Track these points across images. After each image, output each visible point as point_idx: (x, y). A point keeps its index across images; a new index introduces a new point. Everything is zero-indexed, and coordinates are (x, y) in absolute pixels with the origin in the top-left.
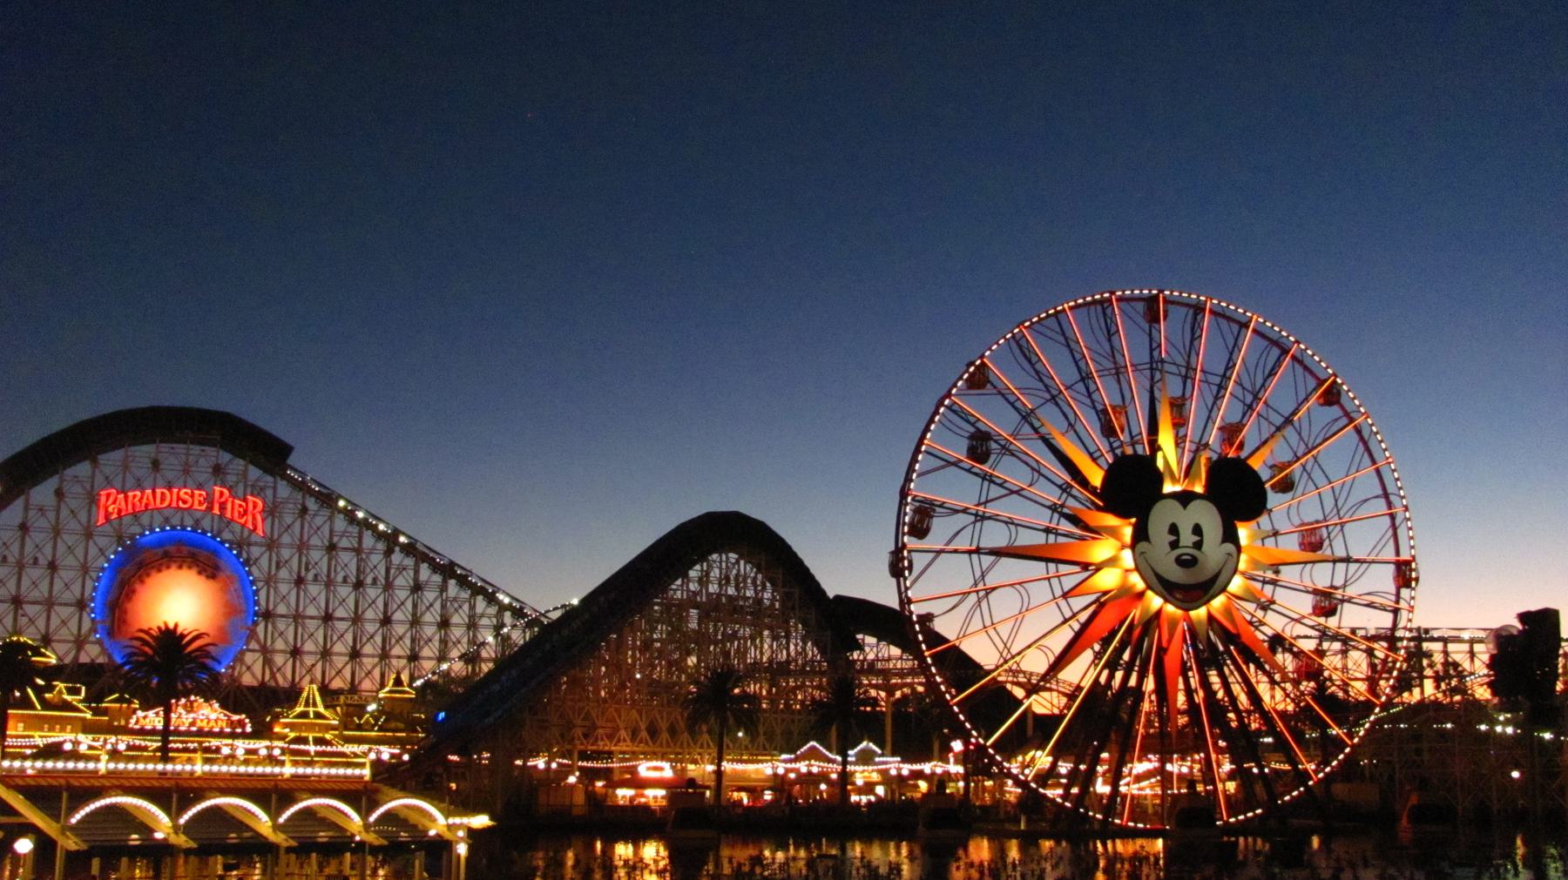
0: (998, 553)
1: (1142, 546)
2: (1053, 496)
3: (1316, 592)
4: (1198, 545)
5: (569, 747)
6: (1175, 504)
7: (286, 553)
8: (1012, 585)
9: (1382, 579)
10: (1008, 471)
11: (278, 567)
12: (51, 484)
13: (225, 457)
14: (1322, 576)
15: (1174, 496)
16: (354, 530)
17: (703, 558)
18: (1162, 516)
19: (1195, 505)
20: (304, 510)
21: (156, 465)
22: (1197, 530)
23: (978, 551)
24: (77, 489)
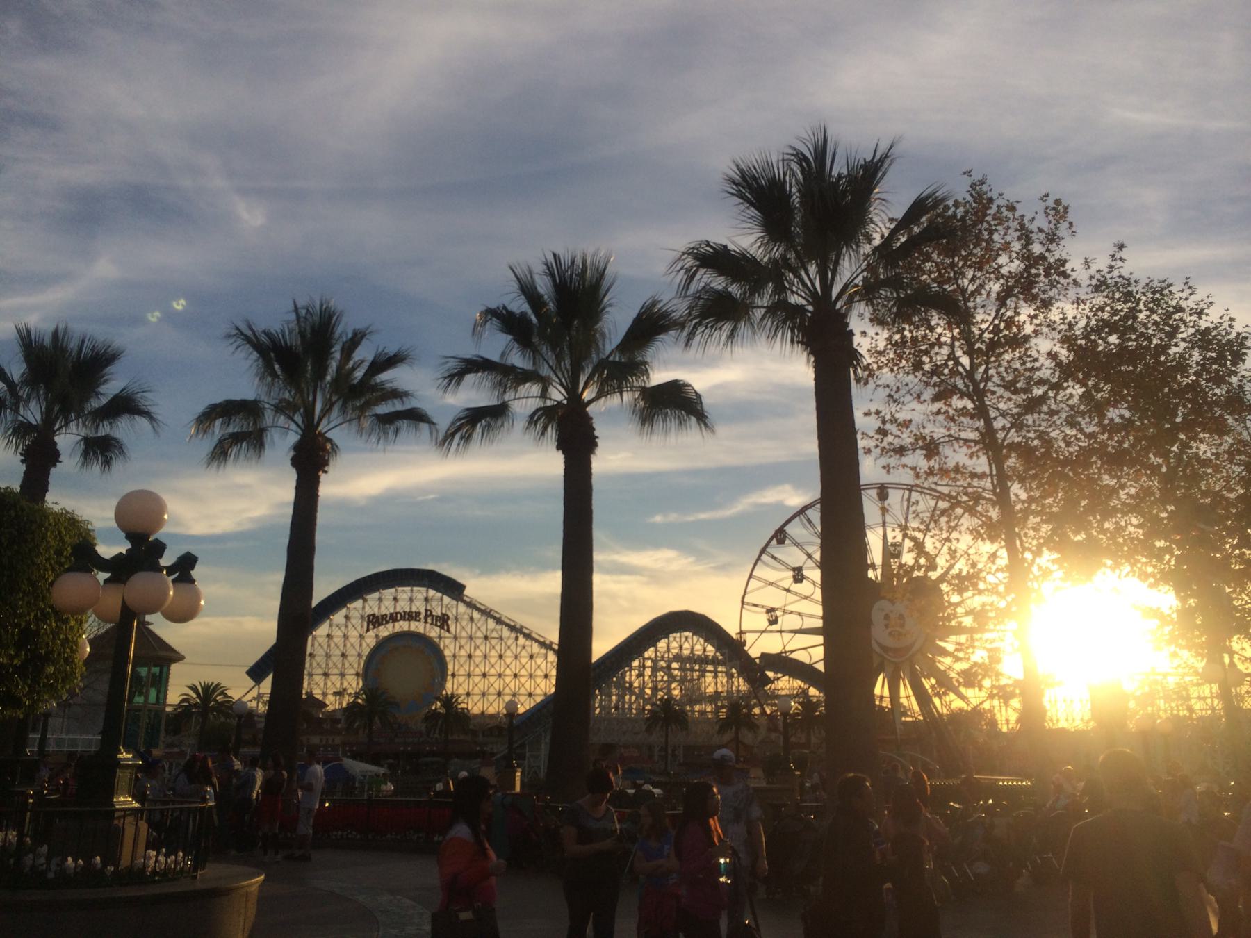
0: (795, 632)
7: (463, 642)
12: (343, 612)
13: (432, 592)
16: (499, 627)
17: (667, 636)
20: (472, 619)
21: (395, 599)
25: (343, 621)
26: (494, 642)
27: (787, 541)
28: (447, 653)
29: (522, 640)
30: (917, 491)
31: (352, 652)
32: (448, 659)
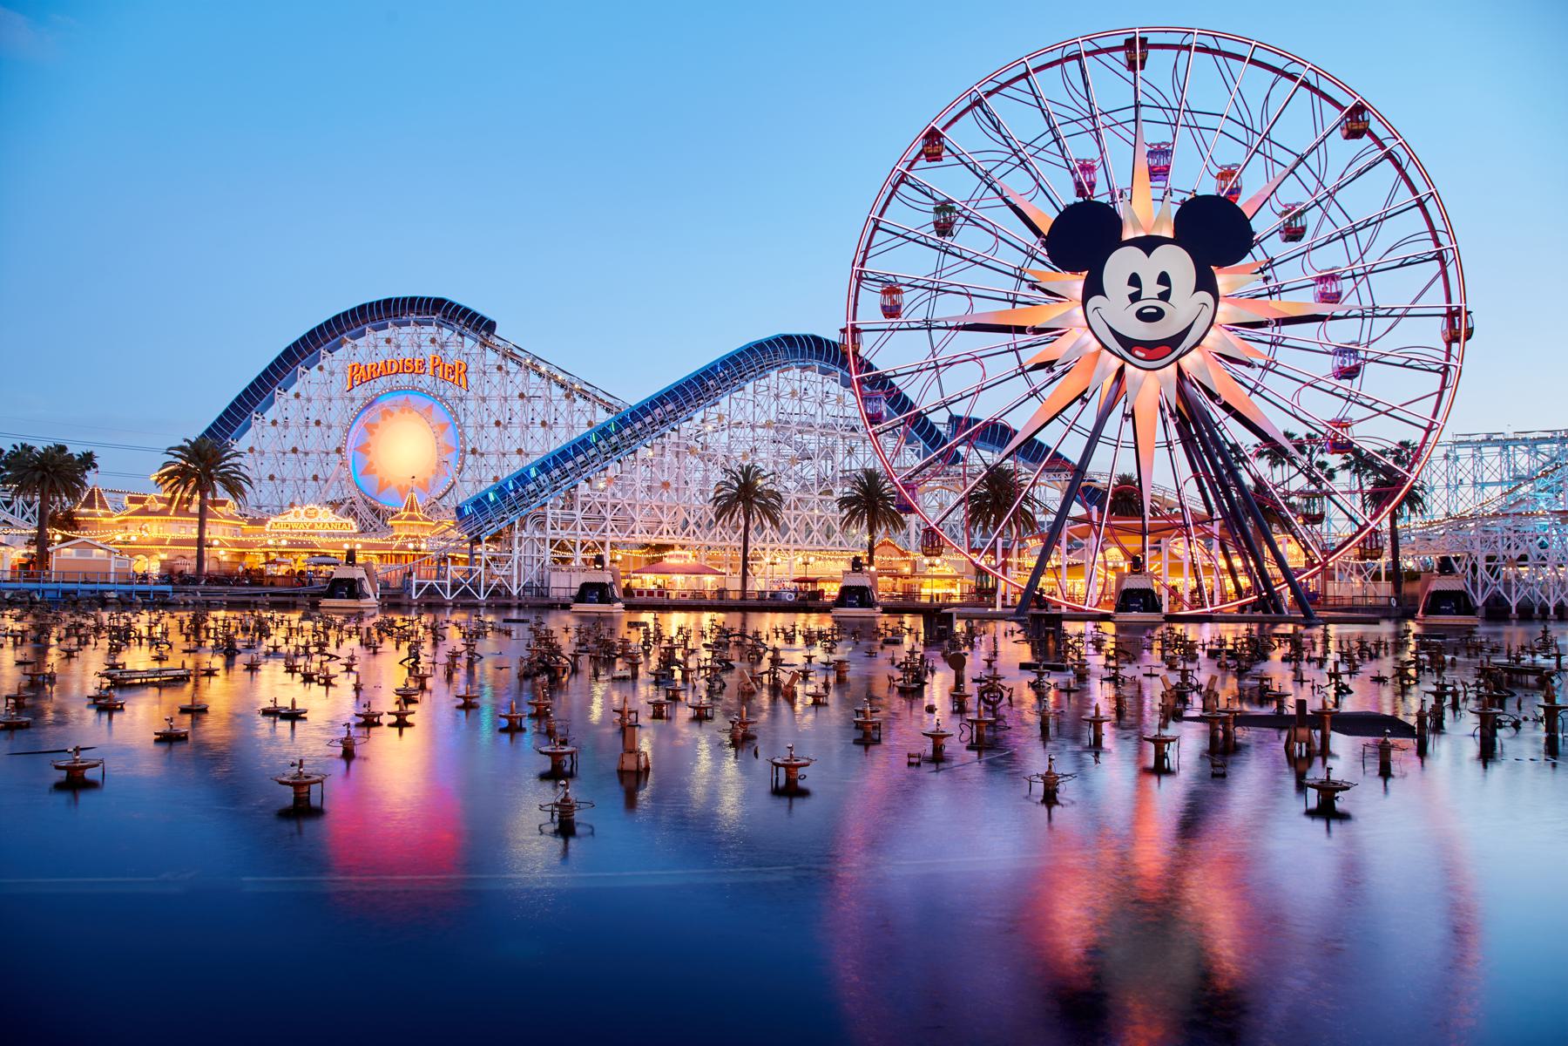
1: (1095, 301)
4: (1165, 296)
5: (602, 539)
6: (1136, 252)
9: (1431, 333)
13: (446, 332)
14: (1342, 333)
15: (1135, 242)
19: (1160, 251)
22: (1164, 279)
29: (580, 402)
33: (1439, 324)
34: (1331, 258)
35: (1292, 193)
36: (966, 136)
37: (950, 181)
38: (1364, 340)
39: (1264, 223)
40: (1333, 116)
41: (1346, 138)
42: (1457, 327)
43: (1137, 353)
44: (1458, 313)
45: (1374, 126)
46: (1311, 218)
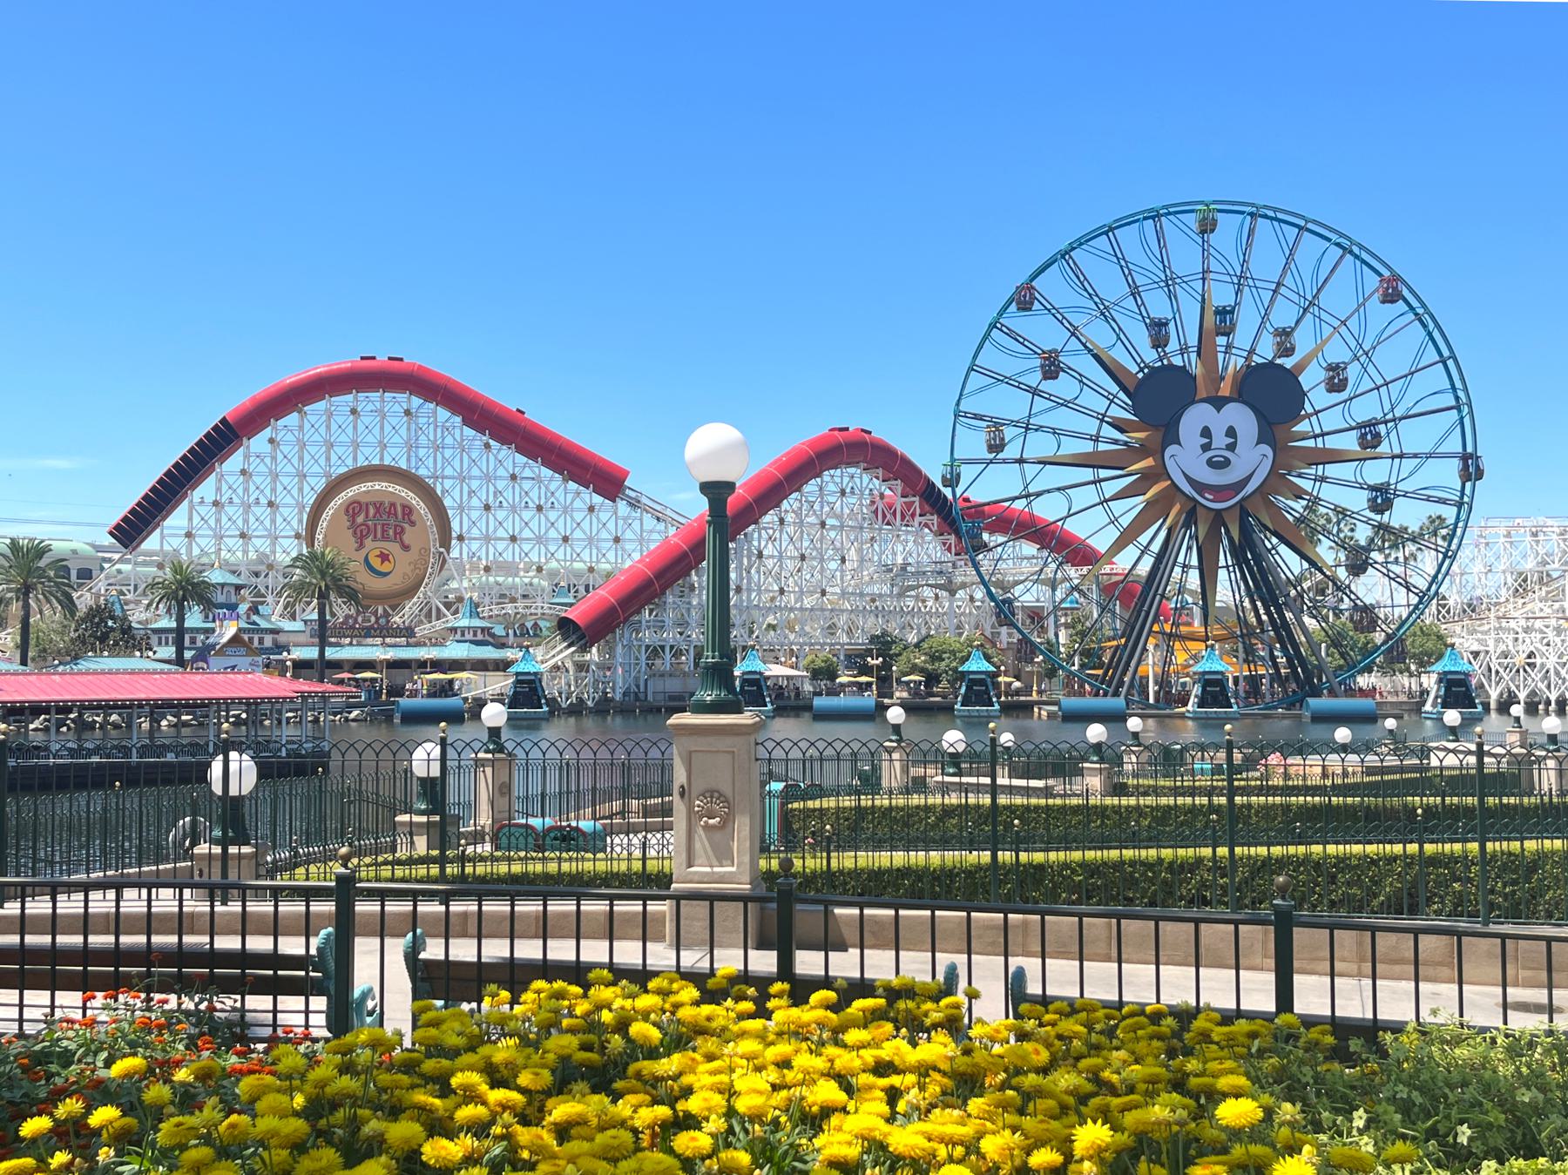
0: (1044, 462)
1: (1171, 450)
2: (1100, 405)
3: (1372, 488)
4: (1231, 447)
6: (1207, 408)
7: (475, 484)
8: (1059, 489)
10: (1063, 386)
11: (470, 497)
12: (267, 433)
14: (1376, 472)
18: (1195, 418)
22: (1231, 432)
23: (1021, 461)
24: (290, 437)
25: (268, 447)
26: (527, 485)
27: (1036, 305)
28: (447, 502)
30: (1265, 217)
31: (283, 499)
32: (450, 513)
33: (1456, 464)
34: (1365, 409)
35: (1337, 352)
36: (1053, 286)
37: (1044, 332)
38: (1393, 481)
39: (1312, 378)
40: (1372, 281)
41: (1383, 302)
42: (1471, 469)
43: (1207, 495)
44: (1471, 456)
45: (1406, 292)
46: (1353, 372)
